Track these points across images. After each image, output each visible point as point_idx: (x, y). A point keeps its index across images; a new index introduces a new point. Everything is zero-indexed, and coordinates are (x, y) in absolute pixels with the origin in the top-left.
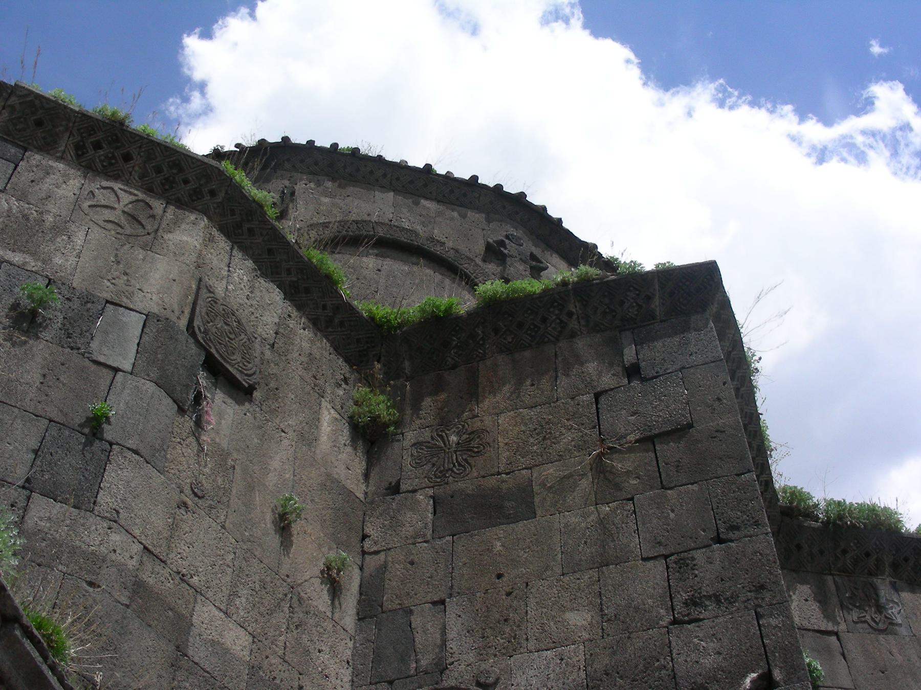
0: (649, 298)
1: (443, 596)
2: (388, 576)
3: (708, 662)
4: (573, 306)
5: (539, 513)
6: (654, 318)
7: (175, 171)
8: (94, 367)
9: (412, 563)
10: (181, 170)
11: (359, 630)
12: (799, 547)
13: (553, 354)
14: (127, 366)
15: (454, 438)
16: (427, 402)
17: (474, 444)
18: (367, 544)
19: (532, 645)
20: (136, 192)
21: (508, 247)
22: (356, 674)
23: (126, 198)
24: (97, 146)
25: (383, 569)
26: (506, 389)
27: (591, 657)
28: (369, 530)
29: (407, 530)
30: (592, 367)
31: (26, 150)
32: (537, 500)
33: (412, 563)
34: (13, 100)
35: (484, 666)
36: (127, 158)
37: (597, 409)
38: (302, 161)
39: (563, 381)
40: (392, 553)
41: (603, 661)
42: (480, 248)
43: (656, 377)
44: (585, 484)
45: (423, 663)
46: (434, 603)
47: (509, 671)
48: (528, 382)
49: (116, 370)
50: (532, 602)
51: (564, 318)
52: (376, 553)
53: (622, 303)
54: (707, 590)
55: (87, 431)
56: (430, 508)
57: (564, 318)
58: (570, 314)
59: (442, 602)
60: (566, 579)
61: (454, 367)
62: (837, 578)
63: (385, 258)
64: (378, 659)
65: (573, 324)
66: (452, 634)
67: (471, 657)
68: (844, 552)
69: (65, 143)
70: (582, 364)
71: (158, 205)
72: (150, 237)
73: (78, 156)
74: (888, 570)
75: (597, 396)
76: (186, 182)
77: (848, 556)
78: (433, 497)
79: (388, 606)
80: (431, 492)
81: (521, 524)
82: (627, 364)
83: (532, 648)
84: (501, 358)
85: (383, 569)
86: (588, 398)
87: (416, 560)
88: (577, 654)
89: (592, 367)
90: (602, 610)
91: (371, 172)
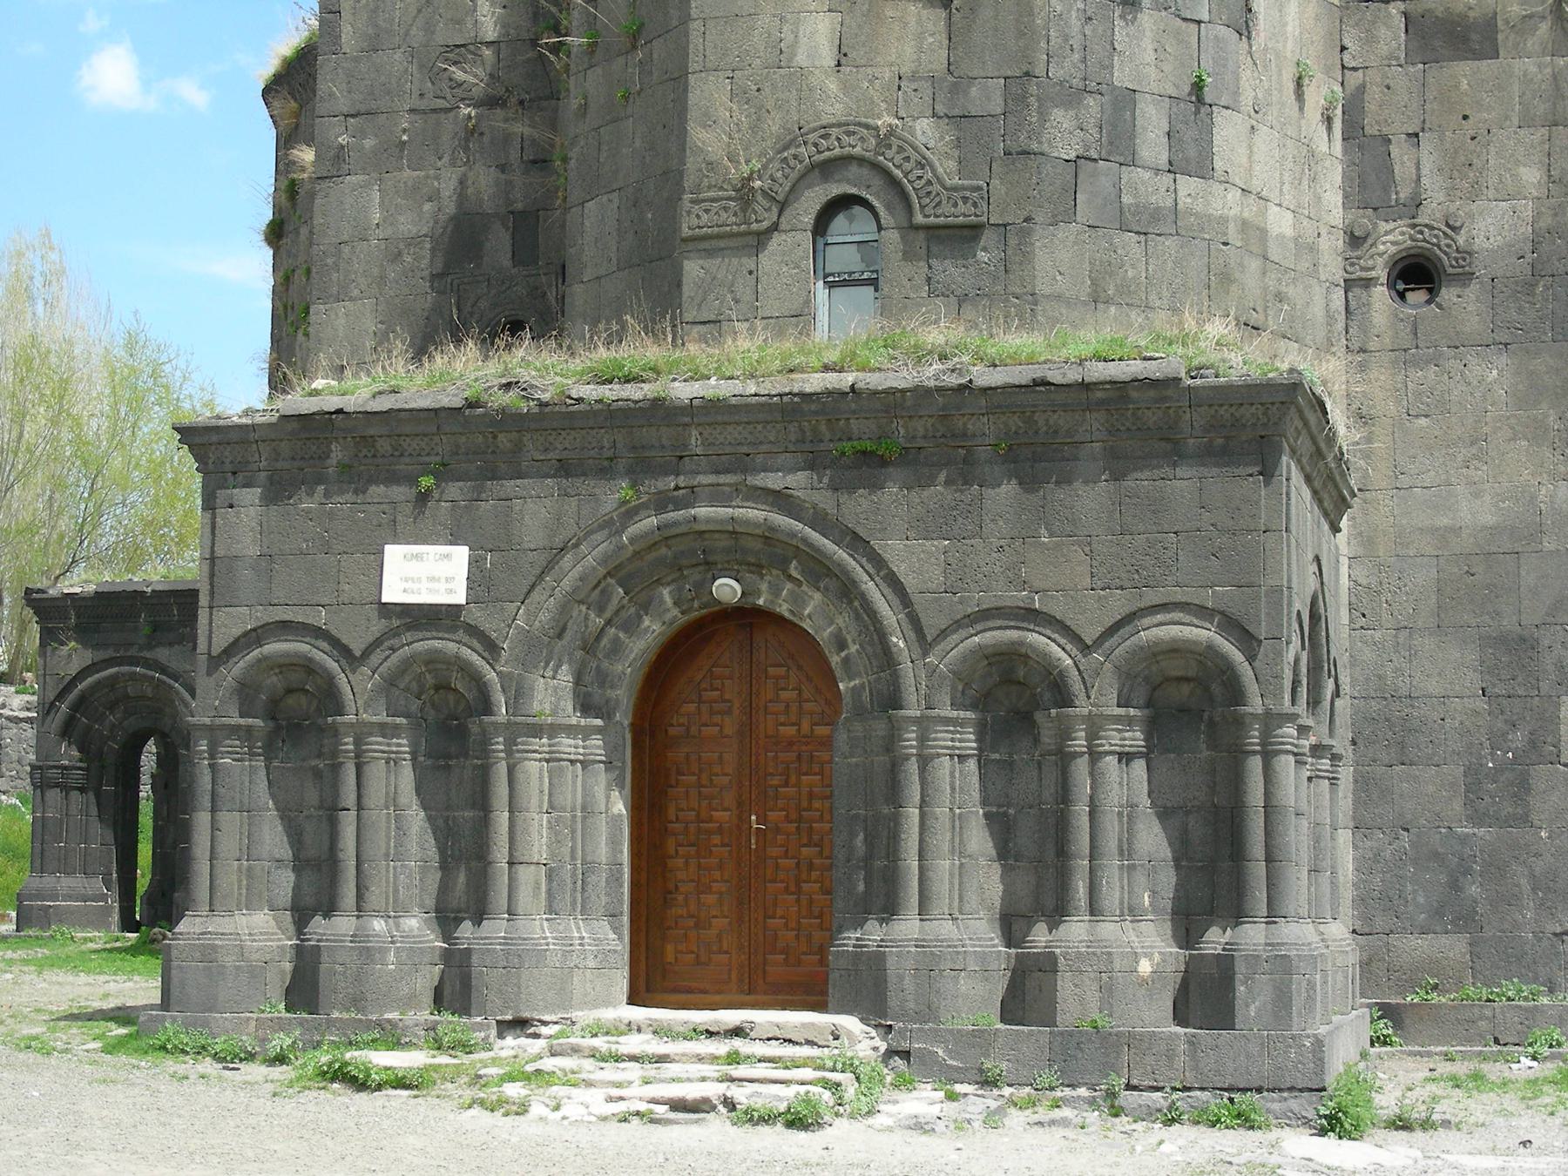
1: (1417, 130)
2: (1366, 97)
5: (1501, 52)
8: (1184, 25)
9: (1388, 88)
11: (1345, 151)
14: (1206, 17)
18: (1346, 57)
19: (1491, 194)
22: (1346, 197)
25: (1362, 89)
27: (1537, 216)
28: (1347, 42)
29: (1383, 49)
32: (1500, 37)
33: (1388, 88)
35: (1452, 208)
40: (1369, 72)
41: (1546, 221)
44: (1544, 27)
45: (1402, 195)
46: (1409, 135)
47: (1471, 216)
49: (1199, 22)
50: (1492, 148)
52: (1355, 69)
55: (1194, 99)
56: (1403, 26)
59: (1417, 135)
60: (1522, 132)
64: (1363, 185)
66: (1425, 171)
67: (1441, 197)
78: (1405, 14)
79: (1368, 131)
80: (1402, 6)
81: (1485, 62)
83: (1491, 197)
85: (1362, 89)
87: (1392, 85)
88: (1527, 209)
90: (1549, 171)
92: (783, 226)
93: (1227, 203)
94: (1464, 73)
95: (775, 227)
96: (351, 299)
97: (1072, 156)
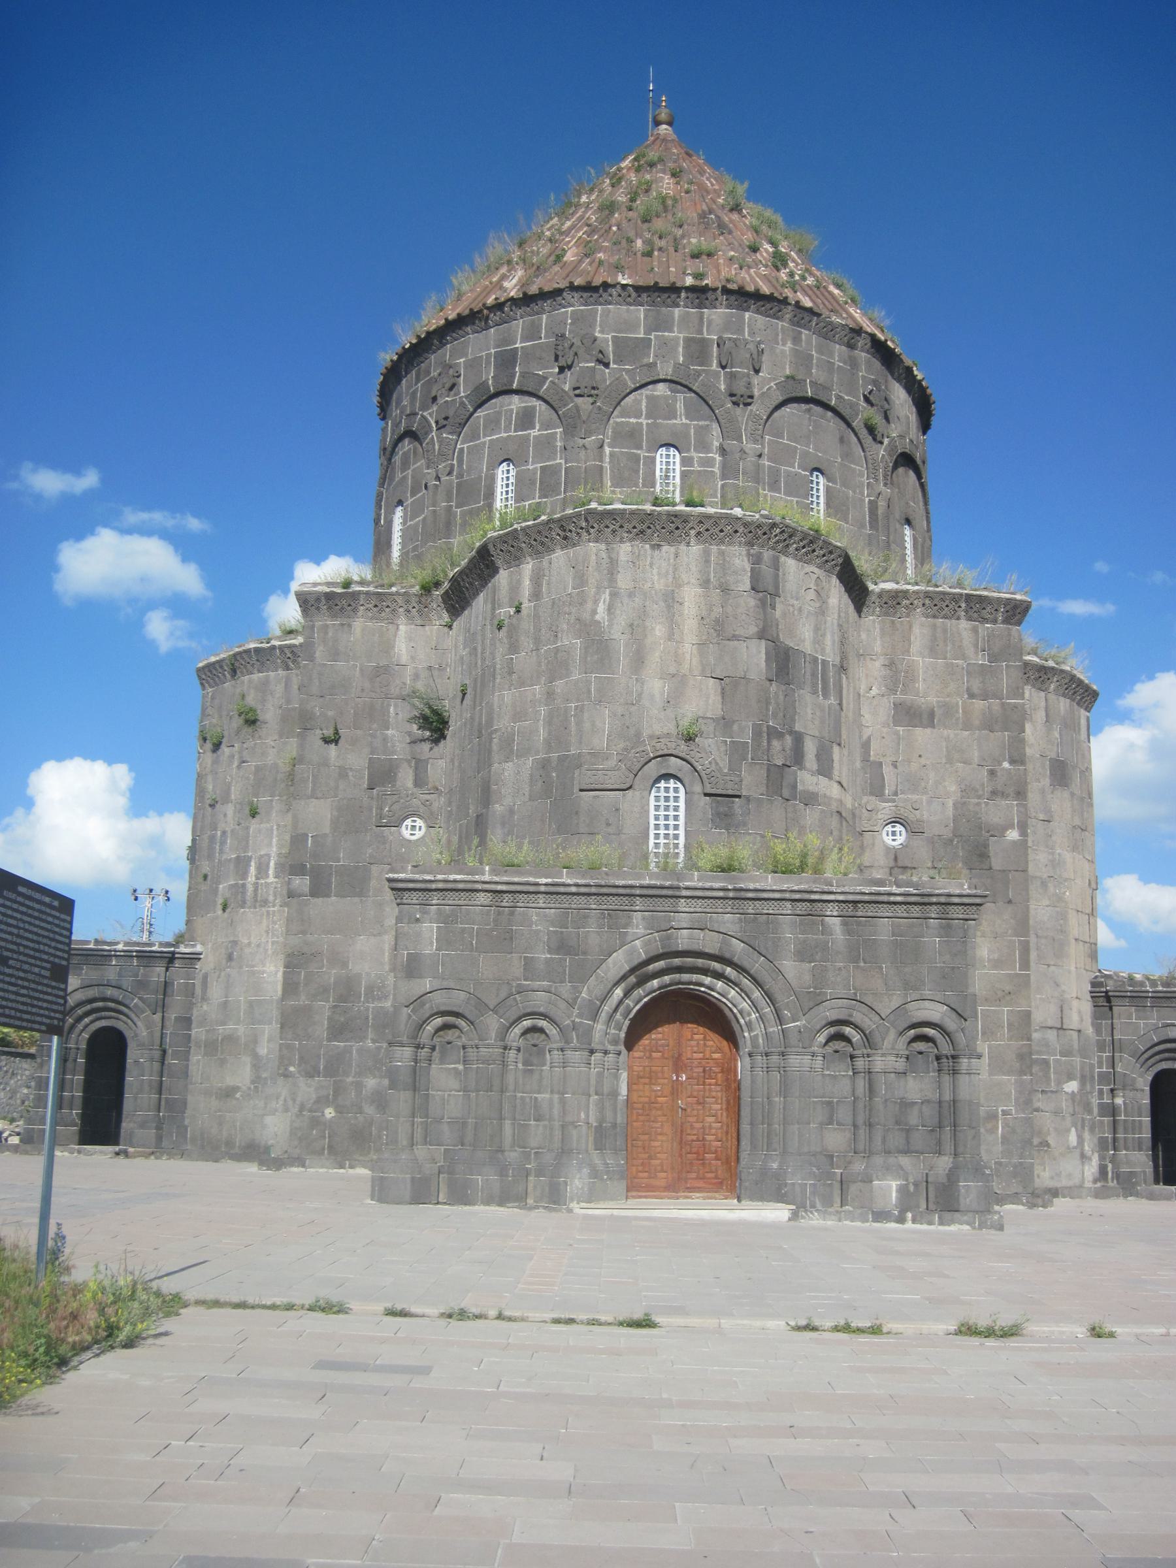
3: (996, 820)
4: (963, 605)
36: (814, 551)
54: (999, 788)
58: (960, 607)
92: (635, 786)
93: (835, 791)
94: (922, 735)
95: (630, 787)
96: (317, 798)
97: (780, 763)
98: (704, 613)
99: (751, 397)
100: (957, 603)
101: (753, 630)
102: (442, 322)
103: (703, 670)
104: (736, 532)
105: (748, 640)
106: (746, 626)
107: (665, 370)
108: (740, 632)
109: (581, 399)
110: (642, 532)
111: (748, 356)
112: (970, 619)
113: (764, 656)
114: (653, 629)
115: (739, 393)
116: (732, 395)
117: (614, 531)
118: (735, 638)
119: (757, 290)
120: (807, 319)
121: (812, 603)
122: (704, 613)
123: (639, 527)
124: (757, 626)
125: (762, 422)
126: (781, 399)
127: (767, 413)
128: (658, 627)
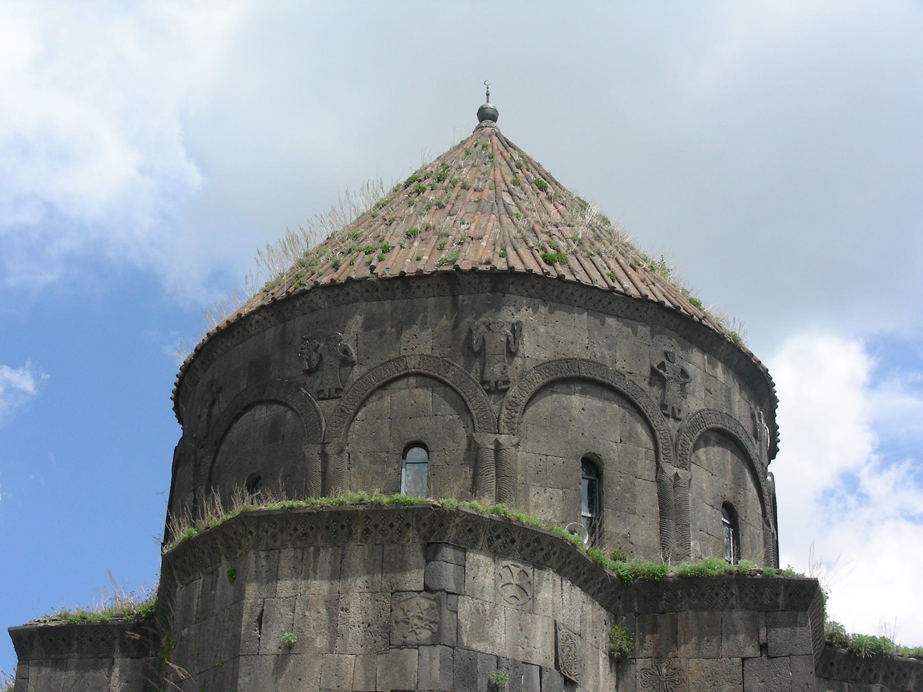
0: (777, 595)
4: (734, 590)
6: (778, 608)
7: (536, 544)
10: (539, 543)
12: (832, 665)
13: (720, 619)
15: (664, 670)
16: (648, 637)
17: (676, 678)
20: (519, 564)
21: (667, 368)
23: (516, 571)
24: (498, 537)
26: (694, 640)
30: (741, 637)
31: (465, 550)
34: (458, 520)
36: (513, 541)
37: (743, 670)
38: (523, 285)
39: (725, 645)
42: (646, 372)
43: (776, 657)
48: (706, 639)
51: (729, 596)
53: (762, 594)
57: (729, 596)
58: (732, 594)
61: (663, 613)
62: (850, 685)
63: (586, 395)
65: (733, 601)
68: (858, 668)
69: (483, 540)
70: (736, 634)
71: (529, 570)
72: (531, 601)
73: (489, 546)
74: (881, 680)
75: (743, 660)
76: (542, 549)
77: (860, 671)
82: (761, 642)
84: (690, 612)
86: (737, 660)
89: (741, 637)
91: (572, 294)
98: (371, 619)
99: (507, 382)
100: (728, 589)
101: (425, 634)
102: (205, 337)
103: (368, 683)
104: (408, 525)
105: (420, 648)
106: (418, 631)
107: (413, 364)
108: (411, 638)
109: (324, 402)
110: (305, 534)
111: (504, 339)
112: (745, 607)
113: (437, 663)
114: (314, 640)
115: (493, 380)
116: (484, 382)
117: (274, 536)
118: (404, 645)
119: (511, 269)
120: (577, 294)
121: (513, 600)
122: (371, 619)
123: (301, 529)
124: (431, 630)
125: (519, 409)
126: (542, 382)
127: (527, 396)
128: (318, 639)
